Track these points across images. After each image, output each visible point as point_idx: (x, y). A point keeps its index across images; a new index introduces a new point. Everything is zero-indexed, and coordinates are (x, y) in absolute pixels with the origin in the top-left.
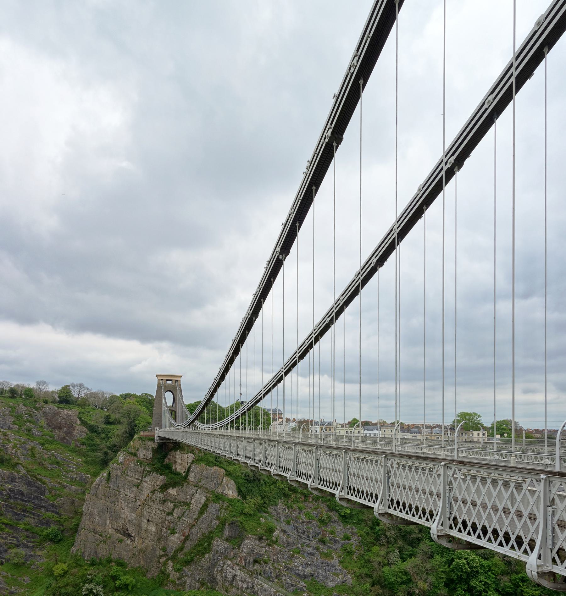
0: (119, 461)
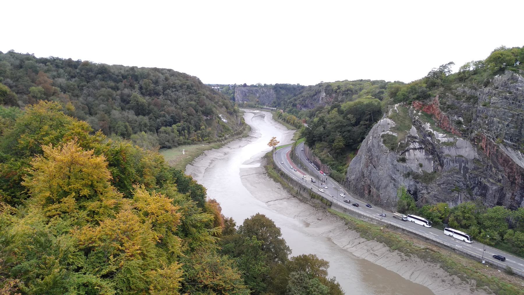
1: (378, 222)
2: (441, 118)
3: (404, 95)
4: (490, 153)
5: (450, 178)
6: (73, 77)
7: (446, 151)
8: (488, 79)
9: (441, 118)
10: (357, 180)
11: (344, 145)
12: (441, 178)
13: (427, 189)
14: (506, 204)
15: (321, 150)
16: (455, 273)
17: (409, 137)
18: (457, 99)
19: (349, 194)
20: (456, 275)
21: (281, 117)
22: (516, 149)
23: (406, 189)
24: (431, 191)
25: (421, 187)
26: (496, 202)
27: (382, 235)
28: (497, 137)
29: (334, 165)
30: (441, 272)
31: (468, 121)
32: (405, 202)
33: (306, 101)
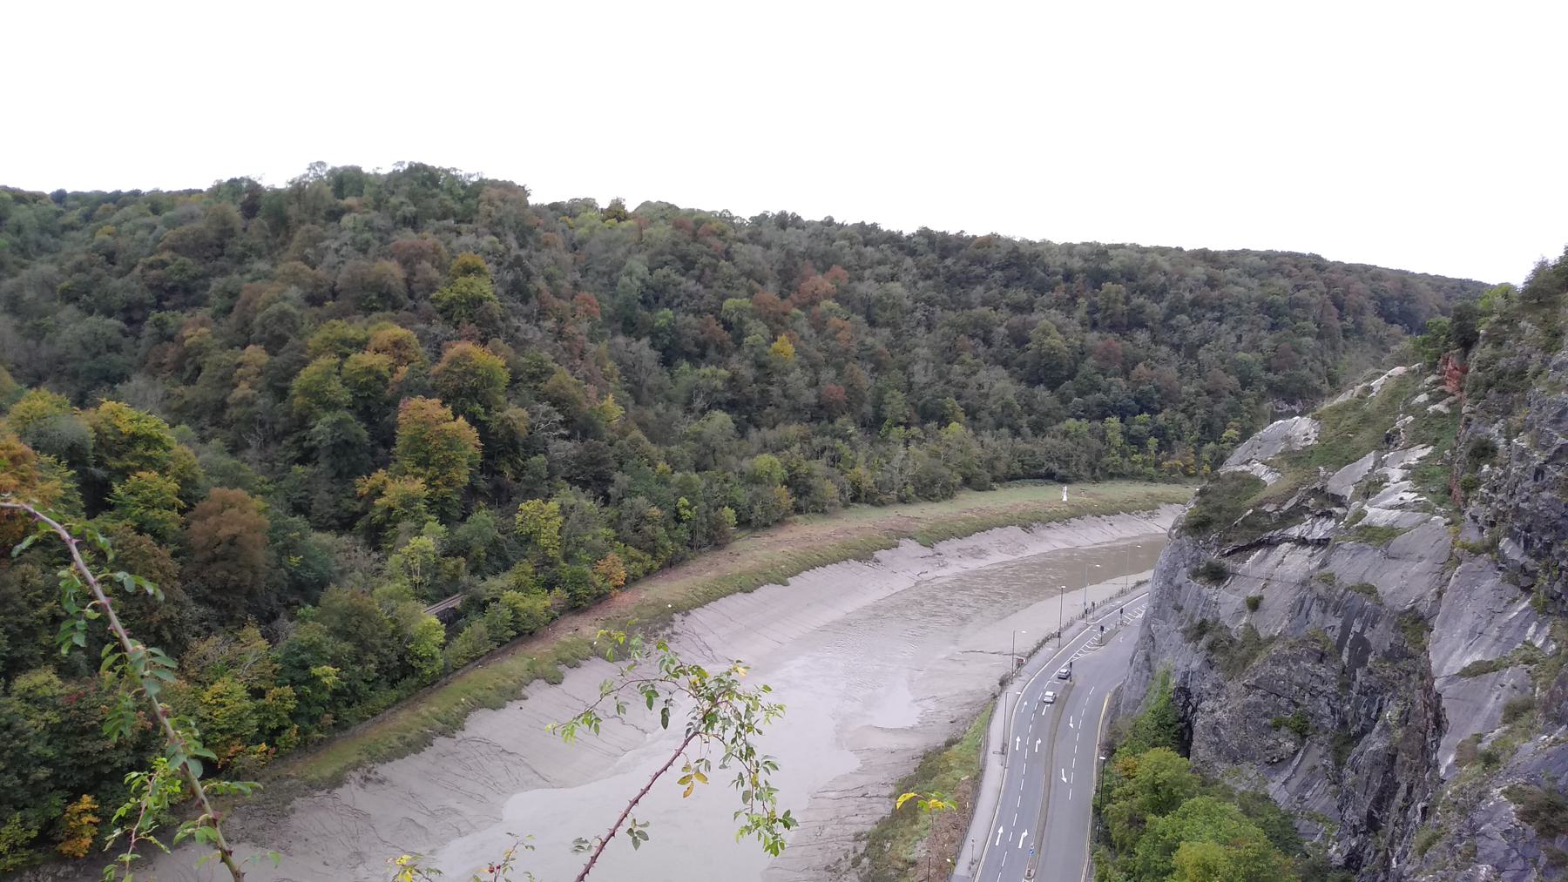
5: (1282, 671)
6: (928, 277)
22: (1523, 589)
23: (1174, 682)
24: (1221, 708)
26: (1365, 811)
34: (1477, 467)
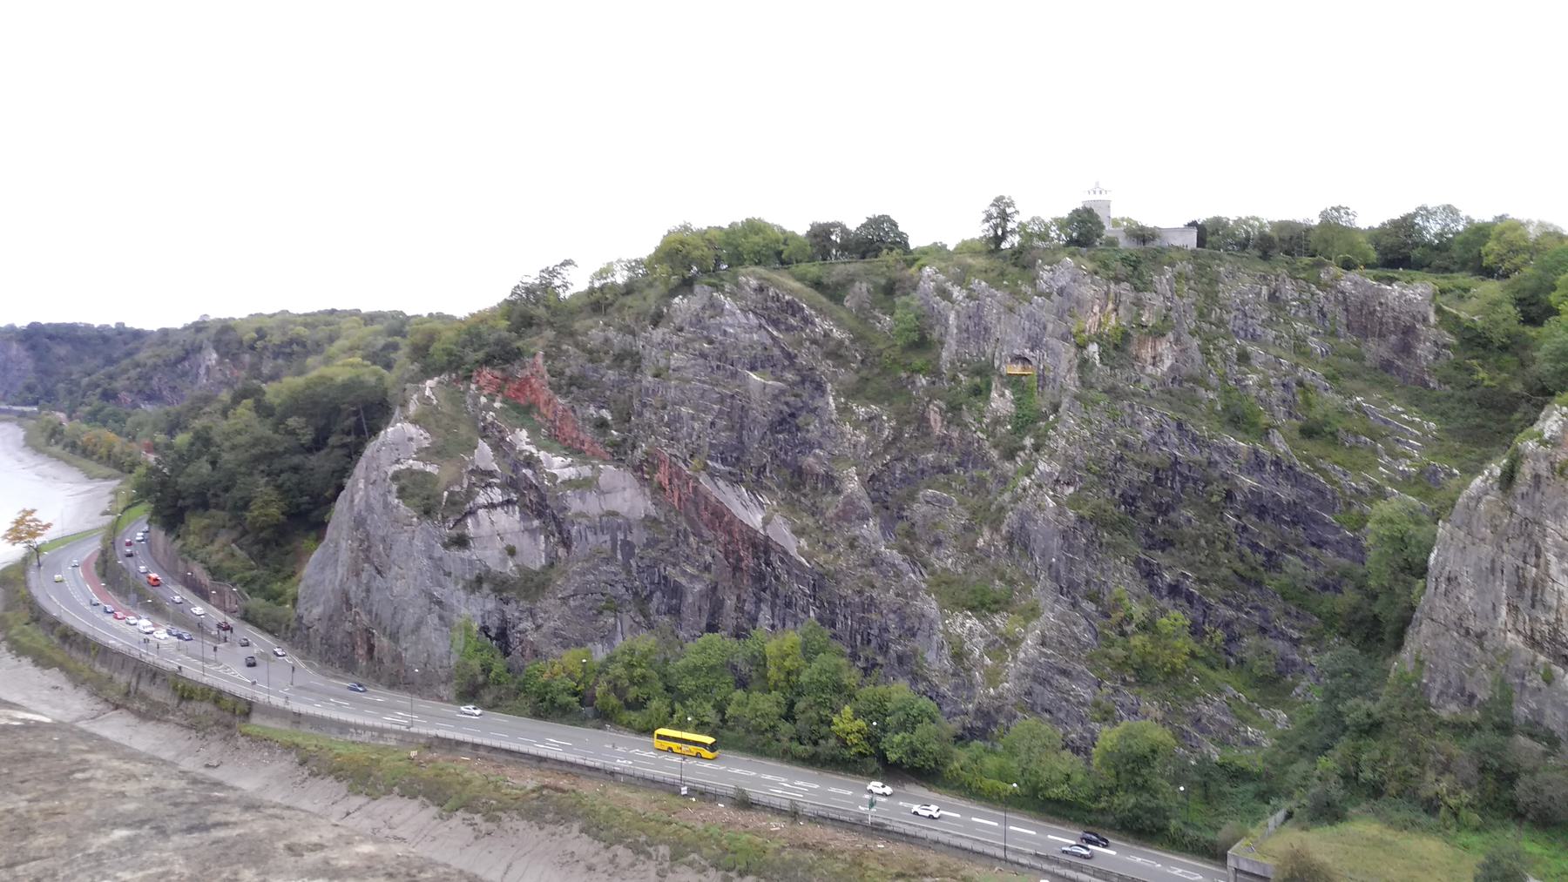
0: (1547, 436)
1: (399, 737)
2: (555, 413)
3: (450, 353)
4: (680, 499)
5: (592, 577)
7: (575, 504)
8: (657, 307)
9: (555, 413)
10: (331, 619)
11: (283, 513)
12: (569, 580)
13: (532, 615)
14: (727, 626)
15: (207, 537)
16: (619, 840)
17: (472, 472)
18: (591, 361)
19: (310, 666)
20: (620, 842)
21: (58, 436)
23: (476, 626)
25: (517, 614)
26: (703, 625)
27: (416, 775)
28: (691, 456)
29: (253, 580)
30: (583, 846)
31: (624, 418)
32: (475, 664)
33: (151, 378)
34: (605, 434)
